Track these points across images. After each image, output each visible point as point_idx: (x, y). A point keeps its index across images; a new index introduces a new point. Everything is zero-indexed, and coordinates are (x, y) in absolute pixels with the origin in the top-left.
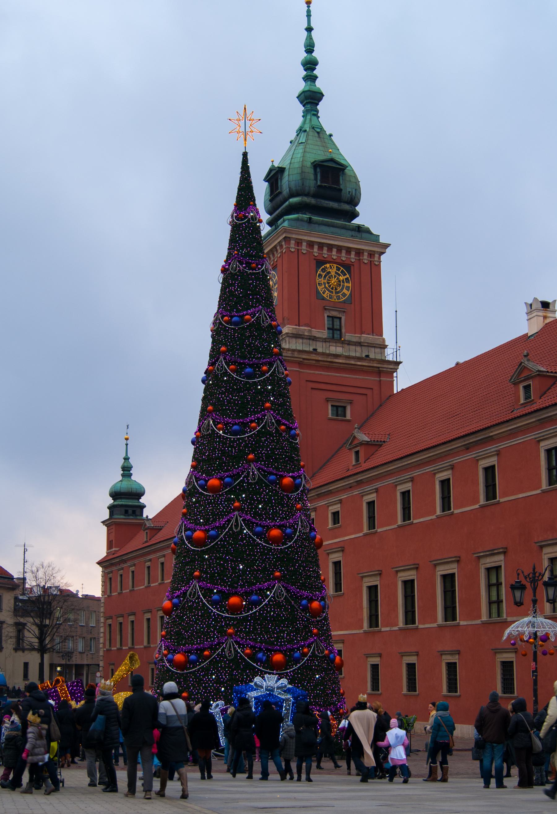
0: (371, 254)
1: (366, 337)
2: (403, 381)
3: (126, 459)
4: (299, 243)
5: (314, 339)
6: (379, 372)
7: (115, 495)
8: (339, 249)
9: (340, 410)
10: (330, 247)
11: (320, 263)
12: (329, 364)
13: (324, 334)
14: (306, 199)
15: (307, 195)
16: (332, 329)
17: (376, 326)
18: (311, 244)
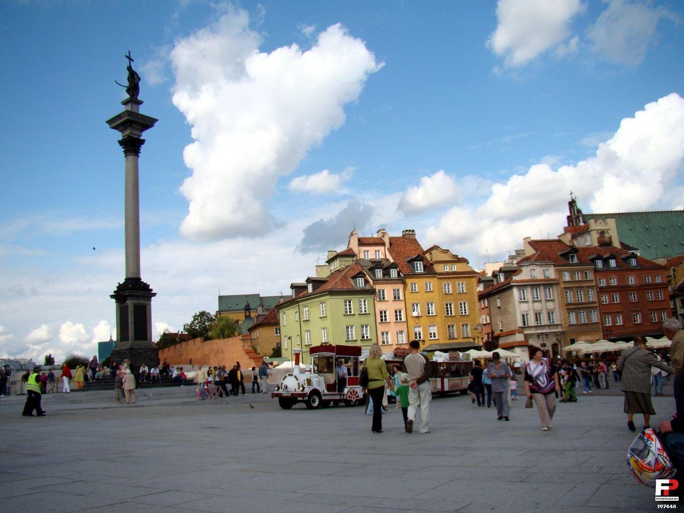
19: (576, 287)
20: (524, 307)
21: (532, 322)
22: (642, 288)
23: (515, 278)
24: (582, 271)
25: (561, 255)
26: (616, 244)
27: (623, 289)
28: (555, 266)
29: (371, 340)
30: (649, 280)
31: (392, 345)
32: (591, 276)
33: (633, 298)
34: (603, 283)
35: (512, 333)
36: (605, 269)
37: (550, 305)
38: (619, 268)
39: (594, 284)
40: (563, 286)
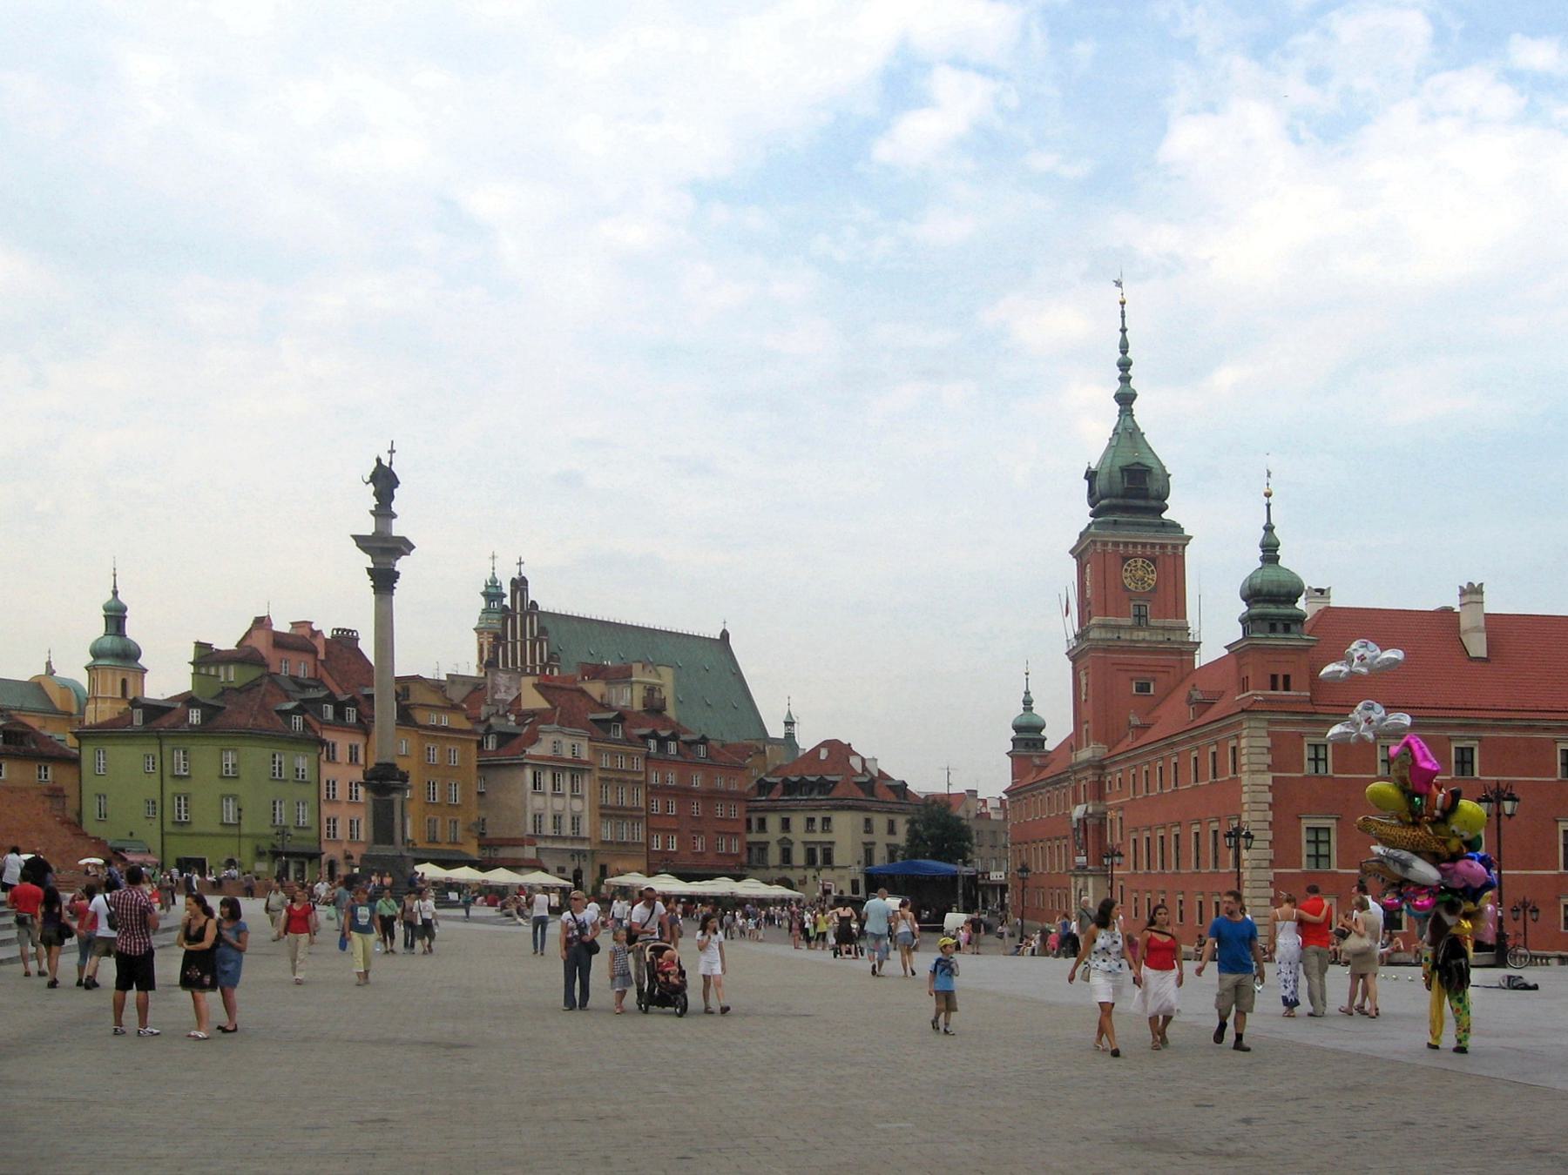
0: (1175, 547)
1: (1169, 622)
2: (1203, 658)
3: (1027, 693)
4: (1105, 544)
5: (1119, 627)
6: (1181, 653)
7: (1017, 728)
8: (1144, 545)
9: (1143, 688)
10: (1135, 545)
11: (1125, 559)
12: (1132, 649)
13: (1129, 621)
14: (1114, 501)
15: (1116, 497)
16: (1139, 616)
17: (1179, 609)
18: (1116, 544)
19: (619, 780)
20: (538, 802)
21: (548, 829)
22: (711, 796)
23: (532, 751)
24: (629, 756)
25: (595, 721)
26: (671, 712)
27: (683, 793)
28: (590, 739)
29: (308, 828)
30: (720, 783)
31: (340, 842)
32: (639, 765)
33: (696, 809)
34: (655, 778)
35: (517, 843)
36: (661, 756)
37: (577, 805)
38: (679, 758)
39: (642, 778)
40: (598, 774)
